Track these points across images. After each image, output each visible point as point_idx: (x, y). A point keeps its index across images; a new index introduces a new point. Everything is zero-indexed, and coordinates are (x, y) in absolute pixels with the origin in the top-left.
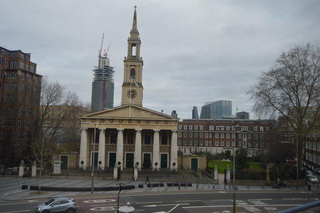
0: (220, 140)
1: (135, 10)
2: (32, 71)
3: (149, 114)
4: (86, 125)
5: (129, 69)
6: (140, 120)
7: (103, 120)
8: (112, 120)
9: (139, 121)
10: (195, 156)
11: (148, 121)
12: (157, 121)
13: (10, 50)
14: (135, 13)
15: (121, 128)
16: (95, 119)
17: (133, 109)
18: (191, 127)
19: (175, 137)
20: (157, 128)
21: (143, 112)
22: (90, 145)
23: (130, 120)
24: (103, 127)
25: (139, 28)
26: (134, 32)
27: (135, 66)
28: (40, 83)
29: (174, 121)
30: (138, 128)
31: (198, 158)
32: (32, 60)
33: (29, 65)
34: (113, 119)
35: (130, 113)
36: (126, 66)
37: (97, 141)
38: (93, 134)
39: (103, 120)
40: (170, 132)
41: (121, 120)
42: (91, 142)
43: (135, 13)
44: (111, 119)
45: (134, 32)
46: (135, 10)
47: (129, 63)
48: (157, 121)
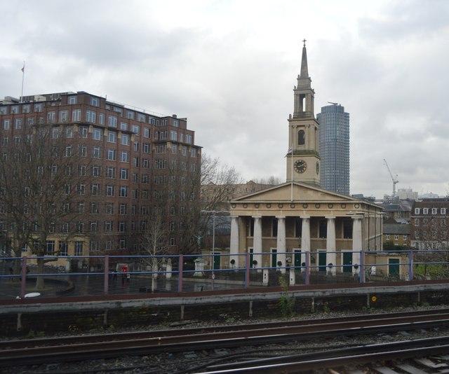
1: (305, 45)
2: (188, 141)
3: (319, 194)
4: (236, 212)
5: (296, 131)
6: (306, 204)
7: (257, 205)
8: (269, 205)
9: (305, 205)
10: (394, 256)
11: (318, 205)
12: (331, 205)
13: (161, 116)
14: (304, 50)
16: (246, 204)
17: (297, 189)
18: (426, 211)
19: (357, 227)
20: (330, 215)
21: (310, 193)
22: (247, 239)
23: (293, 204)
24: (257, 214)
25: (311, 74)
26: (304, 78)
27: (304, 126)
28: (199, 156)
29: (356, 204)
30: (305, 215)
31: (400, 258)
32: (189, 128)
33: (184, 134)
34: (270, 204)
35: (292, 195)
36: (291, 127)
37: (299, 234)
38: (247, 222)
39: (257, 205)
41: (281, 205)
42: (247, 235)
43: (304, 50)
44: (267, 204)
45: (304, 78)
46: (305, 45)
48: (331, 205)
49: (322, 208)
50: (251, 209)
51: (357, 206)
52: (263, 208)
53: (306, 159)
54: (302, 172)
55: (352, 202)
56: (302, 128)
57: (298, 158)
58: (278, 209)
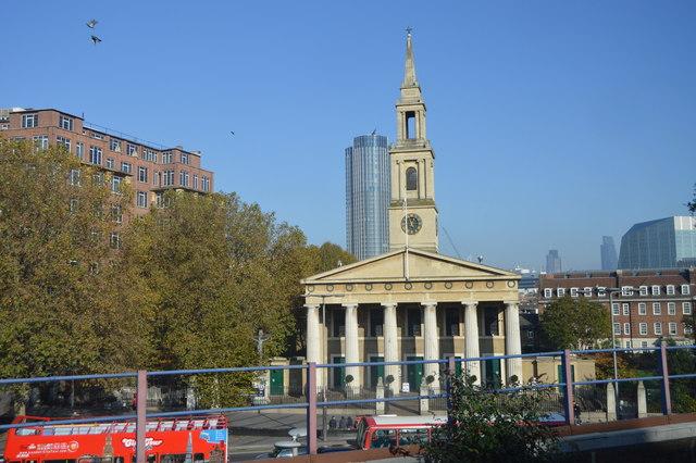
0: (650, 319)
8: (369, 284)
9: (429, 283)
11: (449, 282)
15: (390, 302)
20: (470, 299)
30: (429, 300)
38: (334, 317)
40: (502, 306)
41: (389, 284)
47: (402, 157)
49: (458, 288)
50: (340, 293)
51: (511, 284)
52: (359, 289)
53: (420, 212)
54: (414, 233)
55: (501, 277)
56: (413, 165)
57: (411, 211)
58: (384, 291)
